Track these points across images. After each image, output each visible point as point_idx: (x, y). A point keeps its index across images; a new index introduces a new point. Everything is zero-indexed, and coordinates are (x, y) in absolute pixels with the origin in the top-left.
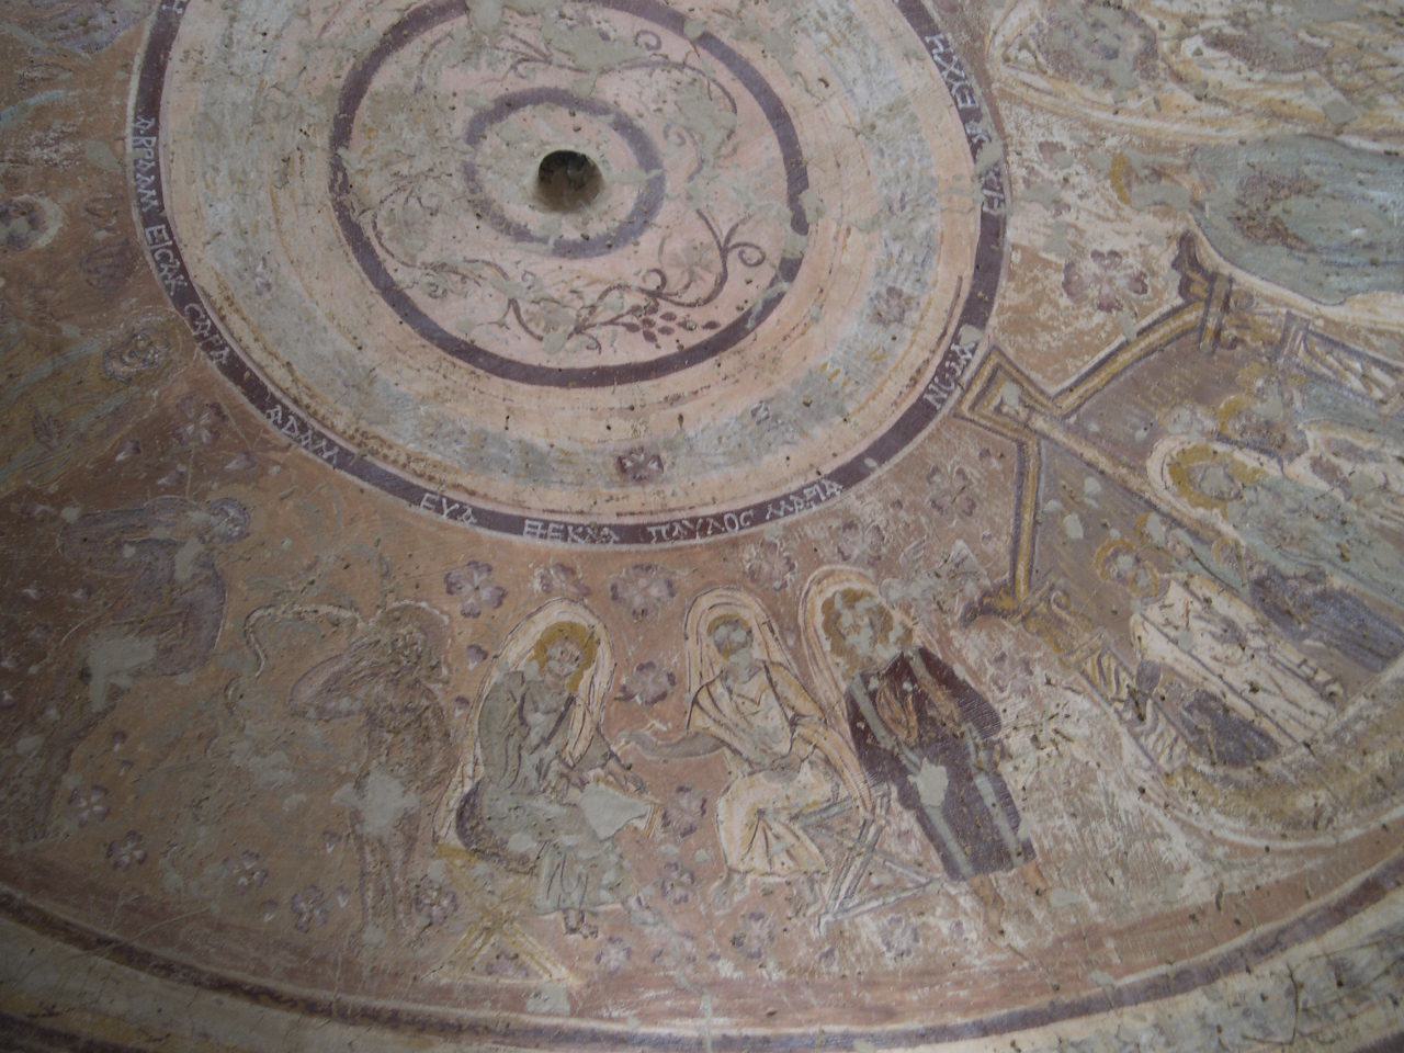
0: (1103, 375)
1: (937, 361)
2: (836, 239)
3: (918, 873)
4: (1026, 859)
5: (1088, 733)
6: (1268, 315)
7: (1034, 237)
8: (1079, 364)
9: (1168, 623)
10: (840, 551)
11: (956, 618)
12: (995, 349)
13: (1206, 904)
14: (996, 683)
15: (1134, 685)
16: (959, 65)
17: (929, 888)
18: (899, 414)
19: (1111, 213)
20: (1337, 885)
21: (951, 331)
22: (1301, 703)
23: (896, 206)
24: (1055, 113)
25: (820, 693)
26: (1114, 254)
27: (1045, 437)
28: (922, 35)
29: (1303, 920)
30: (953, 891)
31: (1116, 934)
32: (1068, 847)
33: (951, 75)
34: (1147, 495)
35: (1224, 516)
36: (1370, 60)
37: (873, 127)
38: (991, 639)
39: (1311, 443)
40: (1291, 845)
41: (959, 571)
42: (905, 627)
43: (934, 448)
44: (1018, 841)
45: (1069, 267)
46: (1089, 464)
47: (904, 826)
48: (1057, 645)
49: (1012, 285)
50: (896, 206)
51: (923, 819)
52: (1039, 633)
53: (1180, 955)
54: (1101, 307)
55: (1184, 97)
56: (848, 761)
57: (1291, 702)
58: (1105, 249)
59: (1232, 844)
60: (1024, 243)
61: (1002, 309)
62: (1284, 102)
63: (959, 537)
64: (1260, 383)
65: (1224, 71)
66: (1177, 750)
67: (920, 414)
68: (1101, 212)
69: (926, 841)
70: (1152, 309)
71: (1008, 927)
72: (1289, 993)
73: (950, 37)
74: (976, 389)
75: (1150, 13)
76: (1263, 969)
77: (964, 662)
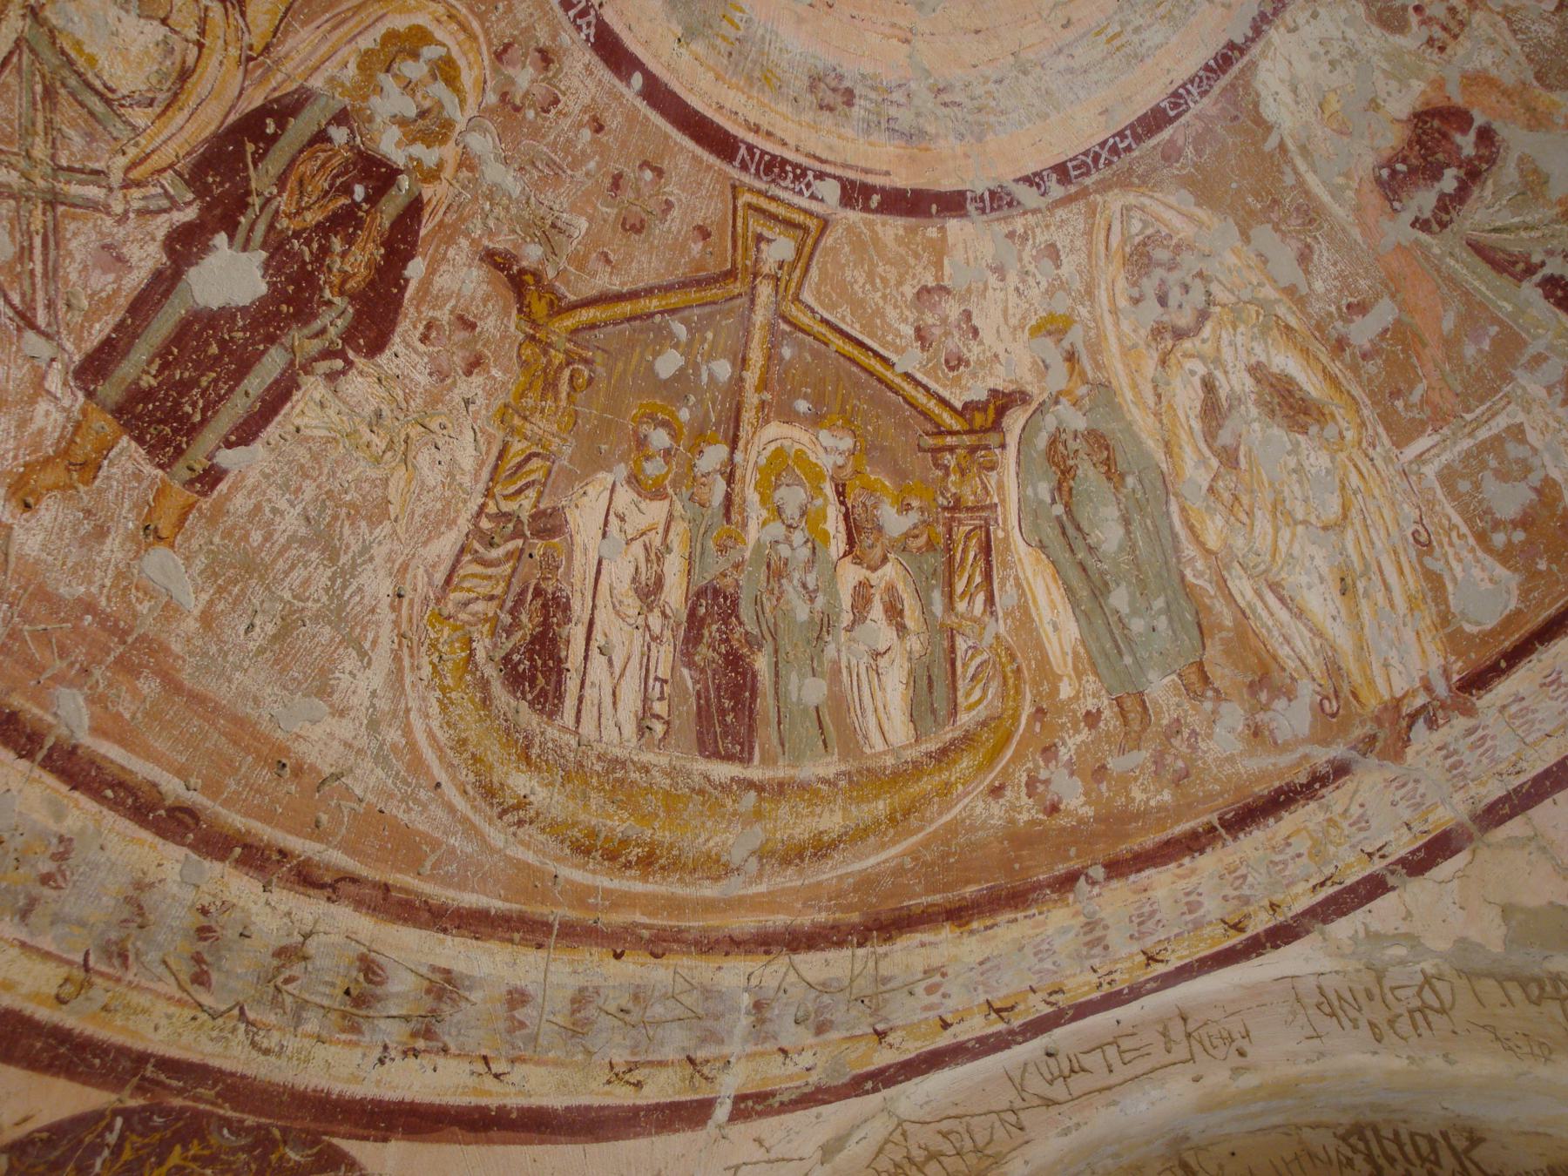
0: (849, 349)
1: (790, 155)
2: (893, 25)
3: (50, 305)
4: (190, 483)
5: (431, 482)
6: (985, 488)
7: (960, 246)
9: (622, 519)
10: (507, 47)
11: (486, 242)
12: (825, 224)
13: (312, 768)
14: (429, 327)
15: (525, 517)
16: (1109, 163)
17: (30, 335)
18: (710, 113)
19: (1013, 321)
20: (462, 886)
21: (828, 169)
22: (620, 705)
23: (946, 97)
24: (1089, 256)
25: (290, 42)
26: (976, 332)
27: (752, 301)
28: (1132, 126)
29: (386, 888)
30: (54, 383)
31: (172, 685)
32: (256, 537)
34: (742, 433)
35: (764, 524)
36: (1245, 499)
37: (1025, 73)
38: (485, 301)
39: (880, 572)
40: (460, 803)
41: (550, 233)
42: (440, 166)
43: (684, 165)
44: (210, 458)
46: (744, 360)
47: (133, 252)
48: (522, 395)
49: (901, 232)
50: (946, 97)
51: (164, 282)
52: (524, 364)
53: (212, 788)
54: (918, 330)
55: (1150, 366)
56: (202, 116)
57: (614, 694)
58: (975, 322)
59: (412, 746)
60: (950, 241)
62: (1181, 447)
63: (591, 220)
64: (915, 504)
65: (1186, 398)
66: (479, 607)
67: (720, 143)
68: (1011, 312)
69: (123, 302)
71: (50, 511)
72: (280, 953)
73: (1136, 154)
74: (772, 207)
75: (1214, 330)
76: (286, 899)
77: (432, 270)
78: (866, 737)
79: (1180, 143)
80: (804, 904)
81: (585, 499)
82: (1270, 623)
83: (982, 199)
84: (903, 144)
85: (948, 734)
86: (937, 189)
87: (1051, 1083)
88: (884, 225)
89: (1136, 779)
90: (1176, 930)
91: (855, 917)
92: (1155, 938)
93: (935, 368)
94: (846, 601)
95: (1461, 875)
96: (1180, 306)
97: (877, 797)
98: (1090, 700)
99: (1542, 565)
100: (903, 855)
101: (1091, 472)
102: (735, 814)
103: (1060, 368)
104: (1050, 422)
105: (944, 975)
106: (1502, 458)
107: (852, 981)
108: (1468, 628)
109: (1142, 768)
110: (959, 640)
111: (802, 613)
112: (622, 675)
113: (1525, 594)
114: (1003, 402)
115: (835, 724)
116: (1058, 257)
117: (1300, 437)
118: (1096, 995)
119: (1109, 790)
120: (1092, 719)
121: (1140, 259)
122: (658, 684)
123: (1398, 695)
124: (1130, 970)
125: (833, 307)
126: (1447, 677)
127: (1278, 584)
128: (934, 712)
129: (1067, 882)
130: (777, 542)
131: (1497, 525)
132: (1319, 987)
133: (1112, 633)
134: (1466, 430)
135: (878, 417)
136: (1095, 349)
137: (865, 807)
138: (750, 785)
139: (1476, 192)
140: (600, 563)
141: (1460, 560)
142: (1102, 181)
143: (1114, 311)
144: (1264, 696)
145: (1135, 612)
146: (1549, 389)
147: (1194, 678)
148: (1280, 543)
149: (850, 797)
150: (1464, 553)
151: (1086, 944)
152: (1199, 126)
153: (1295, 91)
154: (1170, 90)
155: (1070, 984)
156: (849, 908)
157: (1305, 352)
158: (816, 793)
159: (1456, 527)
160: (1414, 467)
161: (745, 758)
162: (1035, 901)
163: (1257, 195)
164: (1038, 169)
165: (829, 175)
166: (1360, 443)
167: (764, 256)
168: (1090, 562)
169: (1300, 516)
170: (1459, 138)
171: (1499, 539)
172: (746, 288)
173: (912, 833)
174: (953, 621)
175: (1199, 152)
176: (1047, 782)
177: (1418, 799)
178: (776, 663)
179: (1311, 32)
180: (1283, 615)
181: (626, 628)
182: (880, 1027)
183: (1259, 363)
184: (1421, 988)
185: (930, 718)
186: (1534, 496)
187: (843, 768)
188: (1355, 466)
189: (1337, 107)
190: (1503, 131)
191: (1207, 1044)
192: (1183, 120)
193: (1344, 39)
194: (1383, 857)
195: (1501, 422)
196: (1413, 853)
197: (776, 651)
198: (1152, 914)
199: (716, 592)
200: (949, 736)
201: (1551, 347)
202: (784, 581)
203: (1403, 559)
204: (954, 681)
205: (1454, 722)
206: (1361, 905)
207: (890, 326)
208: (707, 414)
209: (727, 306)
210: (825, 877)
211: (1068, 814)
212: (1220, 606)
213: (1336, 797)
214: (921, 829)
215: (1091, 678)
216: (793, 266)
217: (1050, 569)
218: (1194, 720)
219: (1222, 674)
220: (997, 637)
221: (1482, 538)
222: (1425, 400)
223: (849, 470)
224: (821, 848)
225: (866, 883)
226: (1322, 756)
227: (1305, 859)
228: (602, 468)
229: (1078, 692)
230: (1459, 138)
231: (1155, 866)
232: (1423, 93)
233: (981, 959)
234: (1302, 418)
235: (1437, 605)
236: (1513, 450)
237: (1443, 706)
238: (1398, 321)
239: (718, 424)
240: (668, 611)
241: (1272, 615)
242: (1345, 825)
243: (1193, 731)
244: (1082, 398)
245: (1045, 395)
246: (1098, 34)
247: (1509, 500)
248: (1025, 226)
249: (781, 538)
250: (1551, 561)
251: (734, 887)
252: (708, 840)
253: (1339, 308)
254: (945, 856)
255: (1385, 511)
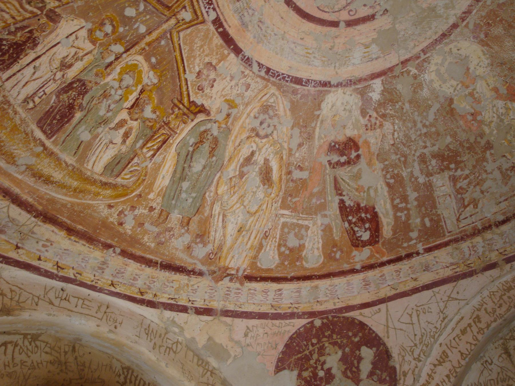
0: (179, 58)
6: (178, 126)
7: (229, 62)
8: (186, 51)
9: (77, 38)
12: (203, 22)
16: (280, 80)
19: (223, 93)
22: (25, 88)
23: (261, 25)
24: (255, 96)
26: (212, 86)
27: (167, 21)
28: (293, 77)
33: (278, 76)
34: (131, 50)
35: (114, 80)
36: (236, 188)
37: (283, 39)
39: (132, 122)
45: (216, 70)
46: (150, 33)
49: (219, 44)
50: (261, 25)
54: (200, 71)
55: (244, 136)
57: (27, 83)
58: (215, 84)
60: (228, 58)
61: (214, 34)
64: (158, 113)
65: (245, 152)
68: (225, 90)
70: (192, 88)
73: (288, 84)
78: (88, 161)
79: (299, 92)
80: (28, 192)
81: (71, 22)
82: (216, 223)
83: (245, 57)
84: (240, 24)
85: (111, 180)
86: (237, 43)
87: (56, 298)
88: (217, 38)
89: (149, 234)
90: (125, 282)
91: (40, 208)
92: (118, 280)
93: (195, 85)
94: (116, 121)
95: (207, 322)
96: (264, 129)
97: (76, 180)
98: (155, 204)
99: (286, 263)
100: (70, 202)
101: (207, 148)
102: (31, 149)
103: (223, 115)
104: (209, 126)
105: (51, 245)
106: (299, 231)
107: (23, 225)
108: (259, 264)
109: (153, 232)
110: (136, 158)
111: (102, 113)
112: (34, 80)
113: (277, 267)
114: (202, 110)
115: (83, 150)
116: (248, 89)
117: (262, 186)
118: (89, 283)
119: (140, 231)
120: (152, 209)
121: (265, 109)
122: (43, 93)
123: (230, 267)
124: (104, 283)
125: (185, 44)
126: (244, 272)
127: (226, 216)
128: (112, 171)
129: (108, 246)
130: (113, 88)
131: (285, 245)
132: (149, 325)
133: (176, 192)
134: (298, 218)
135: (169, 82)
136: (236, 119)
137: (70, 180)
138: (43, 145)
139: (346, 167)
140: (58, 43)
141: (270, 247)
142: (275, 82)
143: (248, 115)
144: (198, 240)
145: (186, 192)
146: (322, 224)
147: (186, 221)
148: (235, 206)
149: (69, 174)
150: (273, 246)
151: (99, 267)
152: (306, 93)
153: (332, 106)
154: (308, 78)
155: (84, 274)
156: (40, 204)
157: (281, 167)
158: (60, 164)
159: (276, 238)
160: (280, 216)
161: (49, 137)
162: (95, 245)
163: (303, 121)
164: (264, 64)
165: (216, 12)
166: (273, 199)
167: (181, 13)
168: (187, 169)
169: (245, 204)
170: (353, 152)
171: (283, 249)
172: (169, 16)
173: (77, 198)
174: (139, 152)
175: (301, 98)
176: (125, 215)
177: (212, 296)
178: (82, 119)
179: (347, 97)
180: (220, 224)
181: (48, 68)
182: (19, 245)
183: (268, 159)
184: (174, 343)
185: (110, 172)
186: (298, 246)
187: (74, 164)
188: (268, 204)
189: (337, 119)
190: (362, 160)
191: (108, 318)
192: (304, 87)
193: (352, 107)
194: (192, 303)
195: (306, 223)
196: (200, 308)
197: (85, 116)
198: (123, 273)
199: (84, 84)
200: (111, 181)
201: (330, 215)
202: (105, 100)
203: (259, 235)
204: (125, 168)
205: (236, 284)
206: (177, 311)
207: (194, 63)
208: (127, 36)
209: (160, 15)
210: (41, 189)
211: (124, 228)
212: (207, 209)
213: (194, 280)
214: (81, 199)
215: (161, 199)
216: (186, 23)
217: (175, 162)
218: (176, 232)
219: (193, 226)
220: (147, 167)
221: (279, 245)
222: (295, 203)
223: (149, 88)
224: (48, 180)
225: (52, 201)
226: (199, 267)
227: (173, 289)
228: (84, 19)
229: (154, 199)
230: (353, 152)
231: (134, 261)
232: (355, 135)
233: (66, 248)
234: (266, 181)
235: (256, 253)
236: (303, 232)
237: (237, 278)
238: (306, 179)
239: (128, 41)
240: (65, 76)
241: (218, 222)
242: (190, 288)
243: (174, 234)
244: (222, 128)
245: (214, 118)
246: (306, 49)
247: (292, 242)
248: (248, 74)
249: (115, 88)
250: (289, 264)
251: (11, 170)
252: (16, 149)
253: (297, 164)
254: (81, 212)
255: (265, 221)
